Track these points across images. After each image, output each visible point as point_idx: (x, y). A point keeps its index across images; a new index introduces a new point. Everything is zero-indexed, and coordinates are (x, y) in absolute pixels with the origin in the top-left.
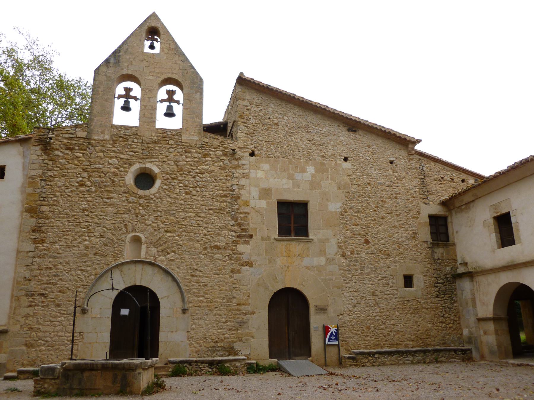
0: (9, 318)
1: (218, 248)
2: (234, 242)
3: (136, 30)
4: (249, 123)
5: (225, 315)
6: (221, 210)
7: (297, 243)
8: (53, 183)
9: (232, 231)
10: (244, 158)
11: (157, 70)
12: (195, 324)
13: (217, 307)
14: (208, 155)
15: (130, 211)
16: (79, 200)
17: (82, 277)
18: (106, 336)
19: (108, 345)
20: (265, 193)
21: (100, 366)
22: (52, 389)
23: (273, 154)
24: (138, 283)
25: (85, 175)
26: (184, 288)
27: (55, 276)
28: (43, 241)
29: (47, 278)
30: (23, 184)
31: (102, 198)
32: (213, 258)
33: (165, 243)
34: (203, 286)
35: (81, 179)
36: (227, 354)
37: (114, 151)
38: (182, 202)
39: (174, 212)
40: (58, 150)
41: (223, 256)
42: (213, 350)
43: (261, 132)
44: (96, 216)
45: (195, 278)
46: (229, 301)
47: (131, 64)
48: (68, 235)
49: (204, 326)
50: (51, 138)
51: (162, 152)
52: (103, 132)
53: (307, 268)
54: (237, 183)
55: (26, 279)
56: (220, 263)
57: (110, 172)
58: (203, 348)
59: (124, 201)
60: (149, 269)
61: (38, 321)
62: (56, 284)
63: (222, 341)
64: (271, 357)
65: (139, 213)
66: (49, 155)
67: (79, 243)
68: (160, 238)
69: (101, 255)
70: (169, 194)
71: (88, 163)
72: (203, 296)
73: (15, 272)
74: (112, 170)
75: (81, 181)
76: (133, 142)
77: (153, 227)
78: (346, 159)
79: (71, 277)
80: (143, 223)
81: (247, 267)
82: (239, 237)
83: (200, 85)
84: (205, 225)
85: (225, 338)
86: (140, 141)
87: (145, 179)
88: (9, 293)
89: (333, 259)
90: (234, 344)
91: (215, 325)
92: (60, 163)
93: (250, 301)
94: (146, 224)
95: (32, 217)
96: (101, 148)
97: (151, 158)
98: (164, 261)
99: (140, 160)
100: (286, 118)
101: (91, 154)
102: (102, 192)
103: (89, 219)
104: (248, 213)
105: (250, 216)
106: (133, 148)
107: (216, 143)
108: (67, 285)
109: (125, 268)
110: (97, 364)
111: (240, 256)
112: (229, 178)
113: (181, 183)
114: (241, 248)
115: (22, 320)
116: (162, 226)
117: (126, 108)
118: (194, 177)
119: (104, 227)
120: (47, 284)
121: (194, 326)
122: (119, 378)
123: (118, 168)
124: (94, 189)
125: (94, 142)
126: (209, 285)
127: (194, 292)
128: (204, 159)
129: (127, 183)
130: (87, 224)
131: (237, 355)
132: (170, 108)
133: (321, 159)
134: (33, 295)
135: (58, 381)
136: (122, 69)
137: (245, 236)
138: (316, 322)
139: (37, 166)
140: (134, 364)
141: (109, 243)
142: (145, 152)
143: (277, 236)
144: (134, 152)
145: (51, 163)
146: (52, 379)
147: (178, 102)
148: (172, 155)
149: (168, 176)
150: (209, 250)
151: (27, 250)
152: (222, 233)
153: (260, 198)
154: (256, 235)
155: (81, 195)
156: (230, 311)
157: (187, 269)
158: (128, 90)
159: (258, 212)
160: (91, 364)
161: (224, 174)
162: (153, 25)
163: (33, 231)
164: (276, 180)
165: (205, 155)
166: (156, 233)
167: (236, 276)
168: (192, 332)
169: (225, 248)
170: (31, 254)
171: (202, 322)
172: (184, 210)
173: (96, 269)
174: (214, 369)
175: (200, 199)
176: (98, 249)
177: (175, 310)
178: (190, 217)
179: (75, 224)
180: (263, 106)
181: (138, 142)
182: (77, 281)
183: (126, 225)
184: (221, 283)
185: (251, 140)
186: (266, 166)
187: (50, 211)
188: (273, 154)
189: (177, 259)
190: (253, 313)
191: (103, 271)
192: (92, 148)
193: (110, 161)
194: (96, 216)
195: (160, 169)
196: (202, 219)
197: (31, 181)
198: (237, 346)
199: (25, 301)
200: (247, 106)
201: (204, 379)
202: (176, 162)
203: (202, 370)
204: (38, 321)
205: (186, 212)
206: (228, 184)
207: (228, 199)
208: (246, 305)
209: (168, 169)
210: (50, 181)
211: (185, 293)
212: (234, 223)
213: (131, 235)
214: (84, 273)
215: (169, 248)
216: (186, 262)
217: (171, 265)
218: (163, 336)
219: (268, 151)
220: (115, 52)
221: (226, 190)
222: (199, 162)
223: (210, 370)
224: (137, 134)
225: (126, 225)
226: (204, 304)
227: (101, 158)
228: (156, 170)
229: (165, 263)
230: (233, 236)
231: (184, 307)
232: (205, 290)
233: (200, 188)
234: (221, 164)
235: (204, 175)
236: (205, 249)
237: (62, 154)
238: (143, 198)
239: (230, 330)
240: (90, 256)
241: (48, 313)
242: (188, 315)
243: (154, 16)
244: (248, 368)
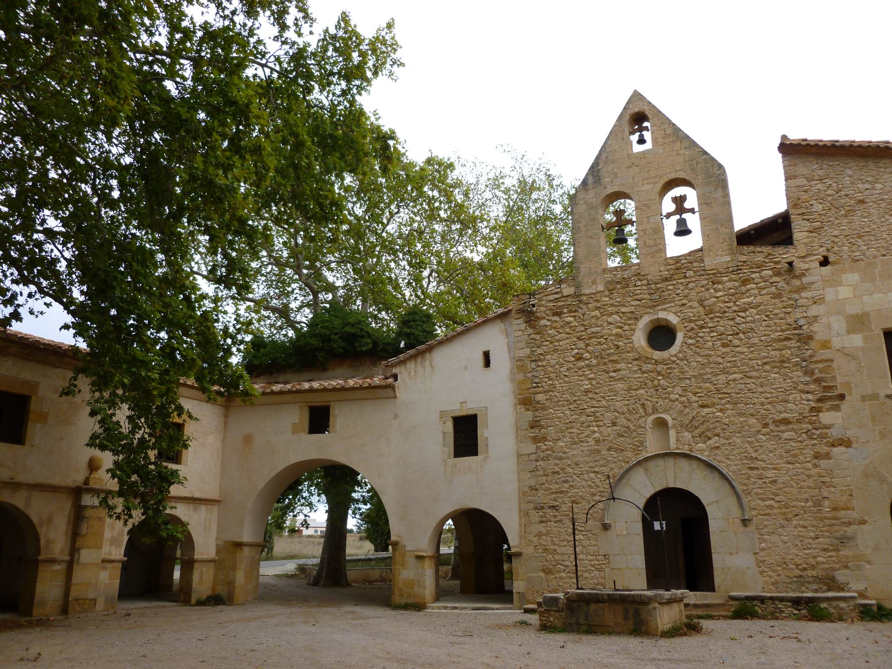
0: (521, 537)
1: (786, 422)
2: (812, 409)
3: (615, 126)
4: (811, 213)
5: (813, 526)
6: (783, 361)
8: (544, 363)
9: (808, 392)
10: (810, 271)
11: (652, 174)
12: (765, 541)
13: (797, 515)
14: (749, 280)
15: (646, 384)
16: (578, 380)
17: (597, 481)
18: (638, 560)
19: (644, 572)
20: (858, 323)
21: (606, 597)
22: (558, 624)
23: (864, 254)
24: (672, 485)
25: (581, 344)
26: (739, 488)
27: (564, 482)
28: (544, 439)
29: (556, 486)
30: (512, 369)
31: (607, 373)
32: (780, 439)
33: (703, 423)
34: (770, 482)
35: (577, 351)
36: (825, 588)
37: (612, 305)
38: (720, 360)
39: (709, 376)
40: (544, 318)
41: (796, 433)
42: (801, 581)
43: (836, 222)
44: (603, 397)
45: (755, 472)
46: (818, 503)
47: (616, 176)
48: (572, 428)
49: (780, 544)
50: (533, 306)
51: (679, 291)
52: (594, 282)
54: (805, 315)
55: (534, 489)
56: (794, 445)
57: (612, 335)
58: (783, 578)
59: (636, 372)
60: (684, 464)
61: (552, 541)
62: (567, 492)
63: (813, 567)
65: (659, 385)
66: (533, 327)
67: (587, 436)
68: (694, 418)
69: (617, 449)
70: (698, 350)
71: (583, 329)
72: (773, 499)
73: (519, 481)
74: (614, 332)
75: (577, 354)
76: (635, 286)
77: (681, 403)
79: (584, 482)
80: (666, 398)
81: (843, 449)
82: (819, 400)
83: (719, 175)
84: (761, 389)
85: (818, 563)
86: (645, 282)
87: (661, 335)
88: (516, 507)
90: (836, 573)
91: (797, 542)
92: (549, 335)
93: (855, 503)
94: (670, 400)
95: (528, 410)
96: (595, 304)
97: (664, 304)
98: (704, 450)
99: (648, 310)
100: (878, 186)
101: (583, 315)
102: (605, 364)
103: (594, 403)
104: (831, 361)
105: (835, 365)
106: (637, 294)
107: (760, 258)
108: (580, 494)
109: (651, 465)
110: (602, 595)
111: (825, 430)
112: (790, 310)
113: (713, 331)
114: (826, 417)
115: (535, 540)
118: (733, 319)
119: (615, 411)
120: (557, 493)
121: (763, 545)
122: (631, 613)
123: (621, 328)
124: (594, 362)
125: (585, 298)
126: (780, 480)
127: (757, 494)
128: (744, 289)
129: (636, 346)
130: (592, 410)
131: (843, 590)
132: (682, 223)
134: (542, 508)
135: (563, 614)
136: (605, 188)
139: (523, 344)
140: (646, 596)
141: (625, 432)
142: (655, 297)
144: (640, 300)
145: (538, 337)
146: (557, 611)
147: (692, 211)
148: (693, 294)
149: (692, 325)
150: (772, 427)
151: (528, 452)
152: (791, 397)
153: (849, 332)
154: (850, 394)
155: (580, 373)
156: (821, 520)
157: (741, 459)
159: (849, 355)
160: (595, 594)
161: (780, 305)
162: (637, 110)
163: (532, 428)
164: (876, 296)
165: (745, 282)
166: (687, 410)
167: (823, 463)
168: (762, 554)
169: (799, 421)
170: (533, 457)
171: (775, 538)
172: (725, 371)
173: (612, 469)
174: (803, 612)
175: (746, 350)
176: (611, 442)
177: (731, 521)
178: (735, 380)
179: (578, 412)
180: (832, 178)
181: (642, 285)
182: (591, 487)
183: (643, 405)
184: (799, 477)
185: (820, 239)
186: (852, 278)
187: (547, 399)
188: (864, 254)
189: (724, 445)
190: (863, 522)
191: (621, 471)
192: (584, 307)
193: (610, 320)
194: (603, 397)
195: (679, 317)
196: (754, 381)
197: (519, 365)
198: (841, 576)
199: (535, 516)
200: (803, 186)
201: (772, 624)
202: (701, 302)
203: (782, 612)
204: (552, 541)
205: (727, 373)
206: (790, 320)
207: (793, 343)
208: (848, 509)
209: (692, 315)
210: (541, 360)
211: (743, 496)
212: (808, 379)
214: (599, 476)
215: (709, 430)
216: (739, 448)
217: (716, 455)
218: (718, 560)
219: (852, 251)
220: (592, 167)
221: (788, 330)
222: (737, 293)
223: (796, 612)
224: (639, 274)
225: (643, 405)
226: (776, 511)
227: (598, 318)
228: (673, 319)
229: (706, 453)
230: (809, 400)
231: (743, 515)
232: (774, 488)
233: (744, 333)
234: (773, 289)
235: (748, 313)
236: (766, 425)
237: (549, 323)
238: (661, 363)
239: (825, 550)
240: (603, 452)
241: (563, 530)
242: (751, 528)
243: (637, 96)
244: (861, 612)
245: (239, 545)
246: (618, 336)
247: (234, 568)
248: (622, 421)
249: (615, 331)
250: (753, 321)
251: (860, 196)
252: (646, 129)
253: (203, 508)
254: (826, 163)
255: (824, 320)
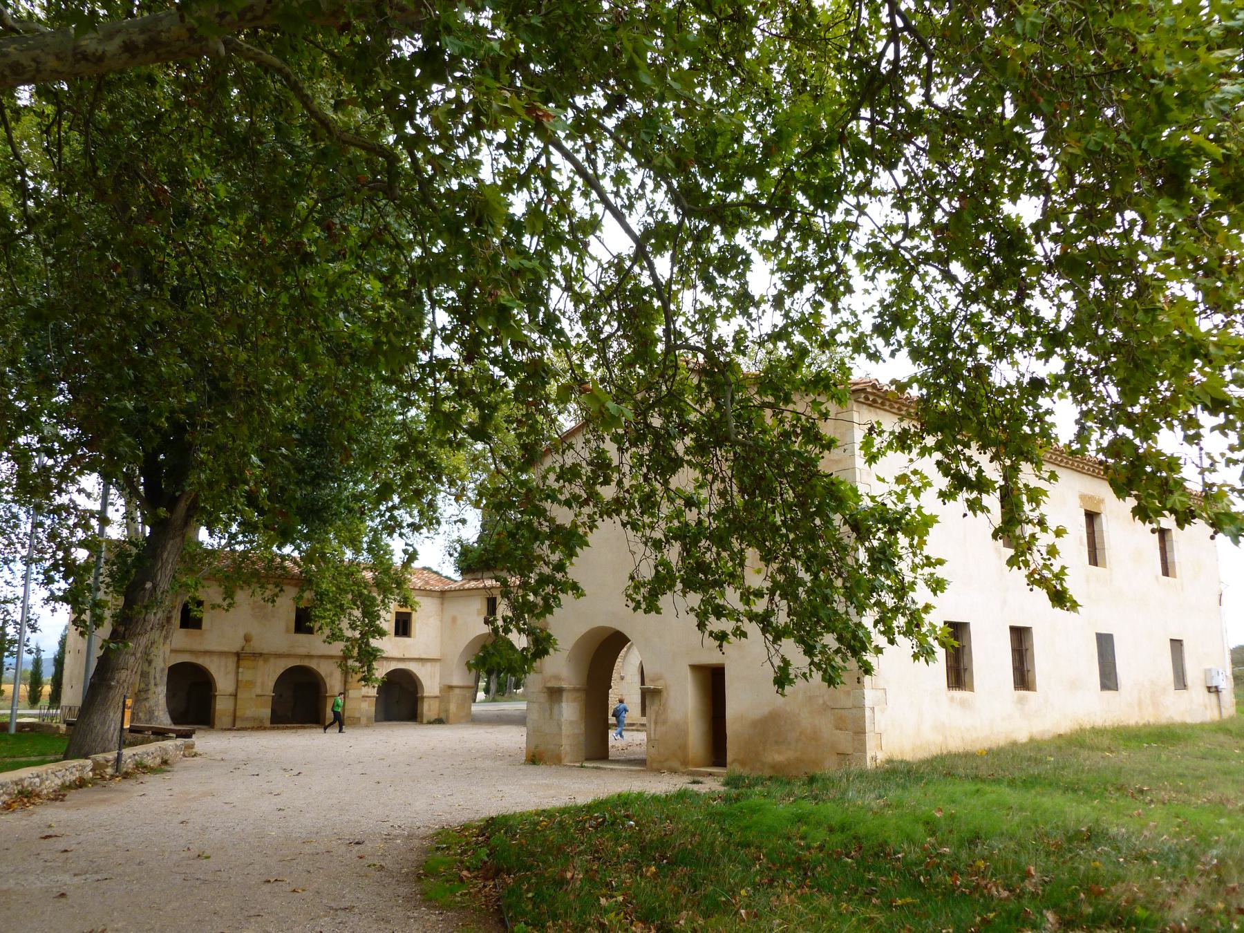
245: (451, 687)
247: (449, 702)
253: (429, 665)
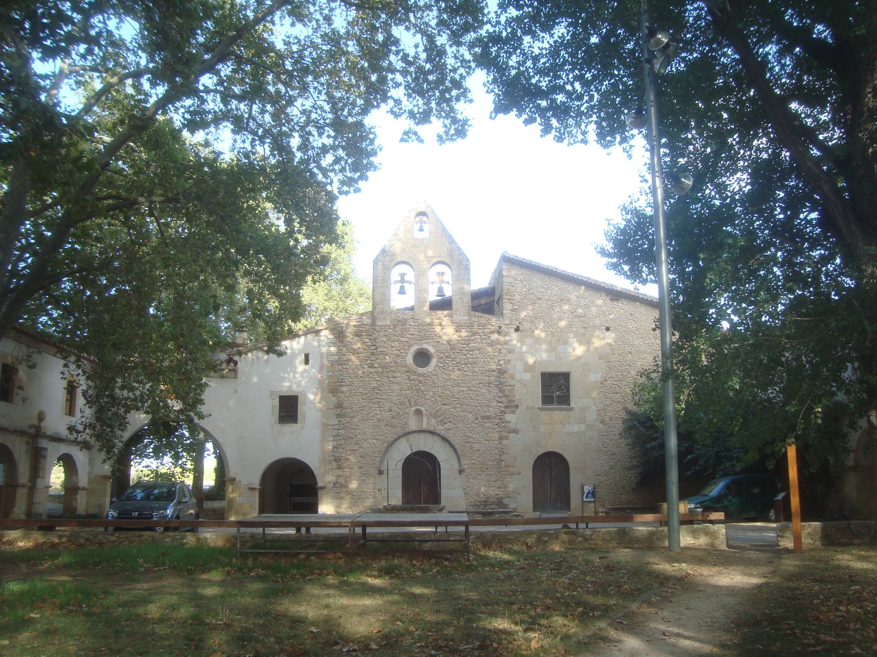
1: (488, 418)
4: (514, 300)
7: (558, 412)
25: (373, 358)
37: (395, 335)
52: (385, 319)
53: (568, 434)
60: (430, 437)
64: (535, 510)
78: (608, 329)
81: (514, 434)
82: (506, 407)
89: (593, 426)
109: (411, 436)
114: (508, 417)
116: (439, 399)
117: (402, 291)
128: (473, 338)
133: (583, 331)
137: (511, 407)
138: (575, 480)
143: (540, 405)
145: (344, 349)
158: (403, 275)
165: (474, 334)
167: (504, 442)
170: (336, 427)
172: (458, 385)
190: (520, 474)
193: (393, 344)
198: (505, 501)
207: (495, 374)
213: (414, 408)
225: (409, 401)
228: (432, 350)
236: (477, 419)
246: (397, 355)
248: (395, 409)
249: (395, 352)
250: (477, 358)
251: (539, 295)
252: (425, 222)
254: (525, 271)
255: (513, 363)
